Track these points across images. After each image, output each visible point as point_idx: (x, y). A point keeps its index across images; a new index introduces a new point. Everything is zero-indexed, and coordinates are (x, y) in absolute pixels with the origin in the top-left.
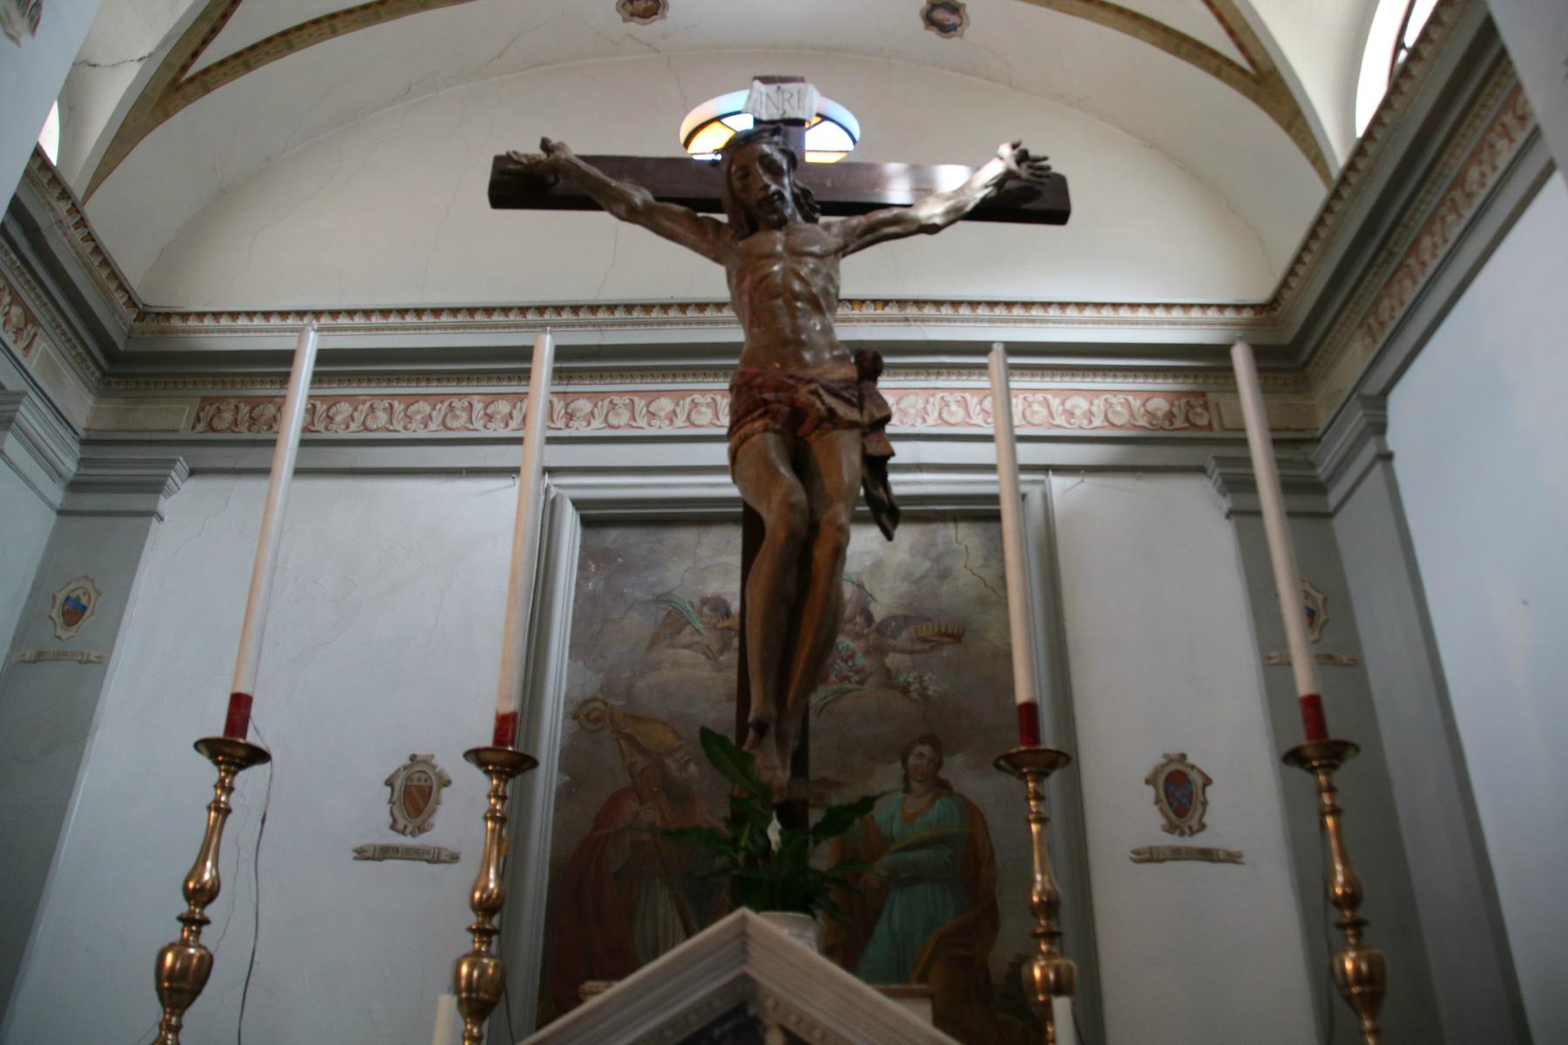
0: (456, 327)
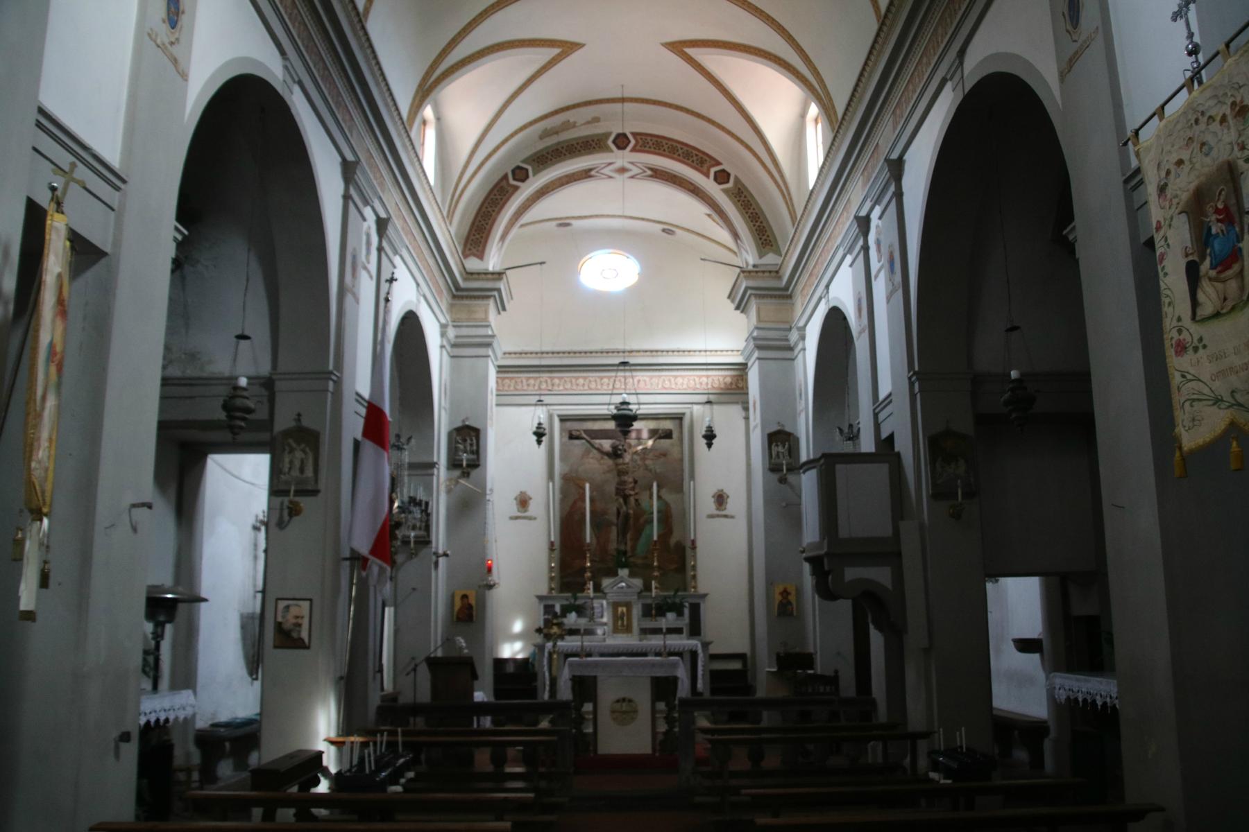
0: (515, 358)
